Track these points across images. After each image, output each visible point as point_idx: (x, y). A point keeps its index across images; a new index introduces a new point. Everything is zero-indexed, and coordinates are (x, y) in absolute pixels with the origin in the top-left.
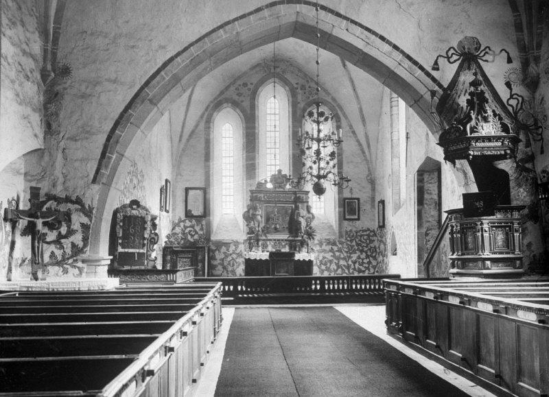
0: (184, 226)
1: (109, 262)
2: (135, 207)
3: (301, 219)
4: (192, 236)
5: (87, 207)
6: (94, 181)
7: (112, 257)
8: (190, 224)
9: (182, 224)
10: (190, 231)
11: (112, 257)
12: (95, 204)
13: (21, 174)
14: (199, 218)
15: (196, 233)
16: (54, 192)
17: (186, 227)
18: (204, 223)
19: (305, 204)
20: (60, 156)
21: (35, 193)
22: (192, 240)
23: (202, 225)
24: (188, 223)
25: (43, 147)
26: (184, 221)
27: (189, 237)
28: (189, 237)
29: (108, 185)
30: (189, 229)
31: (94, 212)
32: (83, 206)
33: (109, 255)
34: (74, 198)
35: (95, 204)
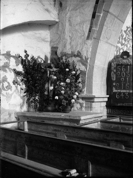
1: (106, 100)
2: (125, 57)
5: (84, 58)
6: (88, 38)
7: (108, 96)
11: (108, 96)
12: (89, 56)
13: (47, 41)
16: (65, 51)
20: (67, 24)
21: (54, 51)
25: (57, 20)
29: (97, 39)
31: (89, 61)
32: (81, 57)
33: (107, 94)
34: (76, 53)
35: (89, 56)
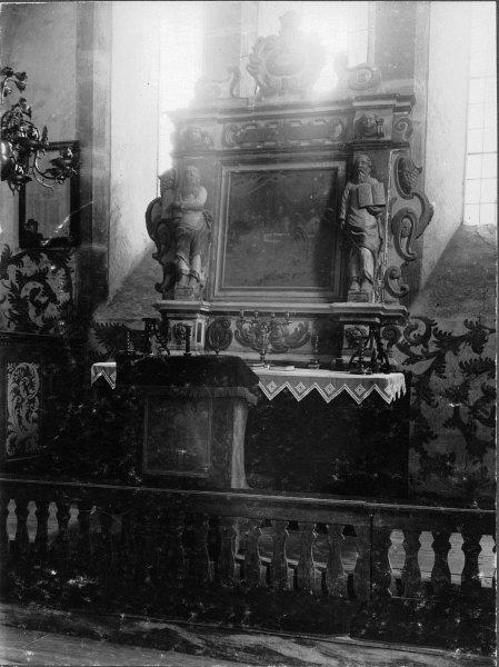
0: (19, 275)
3: (367, 220)
4: (40, 308)
8: (35, 268)
9: (12, 269)
10: (35, 292)
14: (59, 250)
15: (53, 298)
17: (22, 279)
18: (73, 263)
19: (393, 156)
22: (39, 322)
23: (68, 272)
24: (29, 267)
26: (17, 260)
27: (32, 312)
28: (32, 312)
30: (30, 286)
